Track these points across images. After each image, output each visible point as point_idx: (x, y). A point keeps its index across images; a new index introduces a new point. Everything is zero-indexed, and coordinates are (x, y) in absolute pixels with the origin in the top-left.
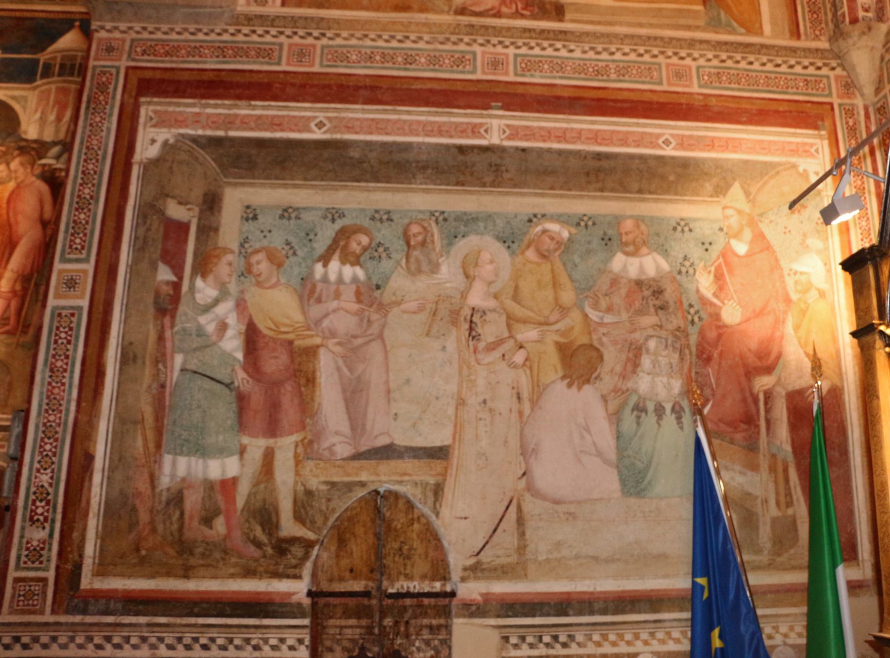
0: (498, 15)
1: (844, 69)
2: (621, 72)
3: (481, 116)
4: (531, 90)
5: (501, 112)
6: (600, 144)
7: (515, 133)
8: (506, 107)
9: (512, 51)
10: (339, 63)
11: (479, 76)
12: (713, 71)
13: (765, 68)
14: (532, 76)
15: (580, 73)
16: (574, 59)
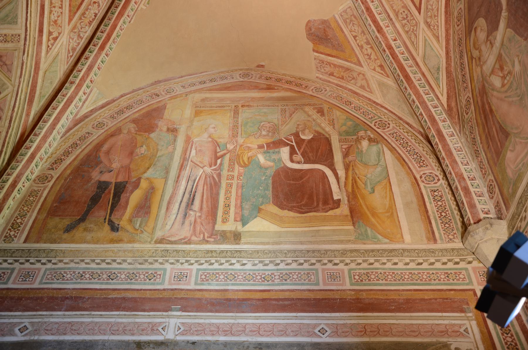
0: (189, 242)
1: (480, 262)
2: (284, 277)
3: (162, 317)
4: (207, 295)
5: (179, 313)
6: (262, 336)
7: (188, 329)
8: (184, 309)
9: (196, 266)
10: (55, 281)
11: (166, 286)
12: (362, 271)
13: (408, 267)
14: (209, 284)
15: (249, 281)
16: (245, 270)
